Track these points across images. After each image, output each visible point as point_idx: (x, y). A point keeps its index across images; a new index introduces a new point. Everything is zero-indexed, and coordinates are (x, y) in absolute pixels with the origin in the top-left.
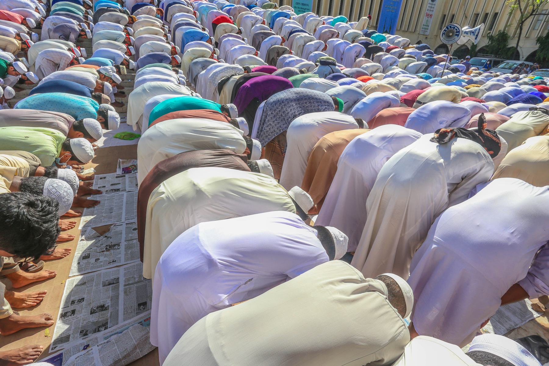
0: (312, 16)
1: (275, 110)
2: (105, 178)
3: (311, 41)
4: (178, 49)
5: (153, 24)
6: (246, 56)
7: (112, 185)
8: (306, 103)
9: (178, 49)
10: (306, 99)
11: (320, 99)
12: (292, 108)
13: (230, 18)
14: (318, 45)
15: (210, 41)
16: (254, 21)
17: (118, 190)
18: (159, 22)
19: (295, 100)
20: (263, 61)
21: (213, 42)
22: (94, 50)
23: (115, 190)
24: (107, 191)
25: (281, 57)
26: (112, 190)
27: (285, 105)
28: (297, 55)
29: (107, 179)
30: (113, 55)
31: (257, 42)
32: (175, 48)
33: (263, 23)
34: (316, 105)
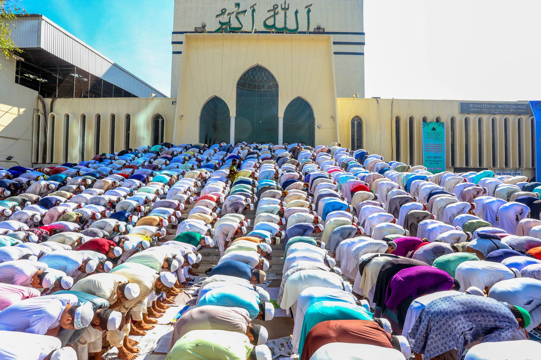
0: (449, 176)
1: (437, 322)
3: (453, 203)
4: (320, 218)
5: (300, 198)
6: (384, 224)
8: (477, 316)
9: (320, 218)
10: (476, 311)
11: (495, 312)
12: (459, 322)
13: (366, 185)
14: (462, 207)
15: (348, 210)
16: (390, 187)
18: (304, 195)
19: (462, 313)
20: (401, 228)
21: (352, 209)
22: (257, 224)
25: (421, 223)
27: (450, 318)
28: (438, 219)
30: (270, 228)
31: (394, 208)
32: (317, 218)
33: (399, 188)
34: (492, 319)
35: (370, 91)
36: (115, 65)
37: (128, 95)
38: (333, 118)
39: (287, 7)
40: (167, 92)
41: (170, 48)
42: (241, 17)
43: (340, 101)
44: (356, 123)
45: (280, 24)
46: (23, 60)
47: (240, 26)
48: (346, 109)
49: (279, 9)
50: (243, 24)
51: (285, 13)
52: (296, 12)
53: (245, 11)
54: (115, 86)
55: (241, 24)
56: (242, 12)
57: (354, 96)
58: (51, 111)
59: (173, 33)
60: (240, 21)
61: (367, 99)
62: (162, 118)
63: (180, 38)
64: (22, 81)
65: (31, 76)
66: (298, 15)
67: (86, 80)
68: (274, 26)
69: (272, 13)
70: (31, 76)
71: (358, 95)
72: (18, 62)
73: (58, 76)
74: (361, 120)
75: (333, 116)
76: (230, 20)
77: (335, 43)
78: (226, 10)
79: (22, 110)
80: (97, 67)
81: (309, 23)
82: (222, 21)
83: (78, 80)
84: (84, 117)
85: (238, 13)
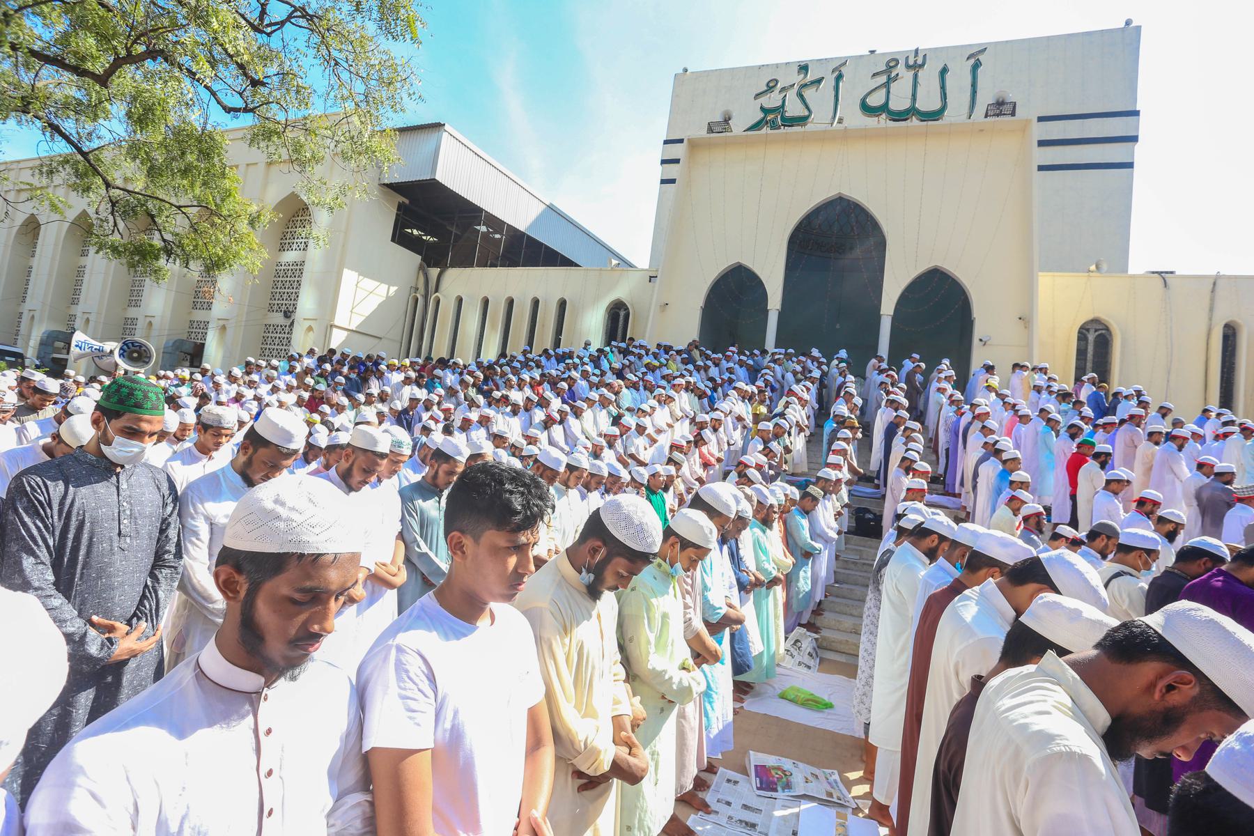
2: (736, 782)
7: (745, 807)
17: (753, 826)
23: (746, 823)
24: (730, 818)
26: (741, 821)
29: (738, 787)
35: (1143, 257)
36: (551, 208)
37: (567, 262)
38: (1026, 320)
39: (920, 61)
40: (641, 259)
41: (658, 172)
42: (809, 94)
43: (1046, 282)
44: (1091, 337)
45: (899, 102)
46: (407, 201)
47: (806, 113)
48: (1066, 303)
49: (901, 68)
50: (811, 106)
51: (916, 76)
52: (944, 71)
53: (819, 81)
54: (547, 247)
55: (807, 107)
56: (813, 83)
57: (1093, 268)
58: (437, 291)
59: (666, 142)
60: (808, 101)
61: (1133, 276)
62: (627, 309)
63: (677, 151)
64: (400, 237)
65: (415, 232)
66: (948, 76)
67: (497, 236)
68: (884, 108)
69: (883, 79)
70: (415, 232)
71: (1105, 267)
72: (400, 207)
73: (454, 230)
74: (1107, 329)
75: (1030, 317)
76: (784, 102)
77: (1042, 143)
78: (777, 81)
79: (393, 289)
80: (518, 213)
81: (974, 92)
82: (766, 106)
83: (485, 235)
84: (486, 302)
85: (805, 85)
